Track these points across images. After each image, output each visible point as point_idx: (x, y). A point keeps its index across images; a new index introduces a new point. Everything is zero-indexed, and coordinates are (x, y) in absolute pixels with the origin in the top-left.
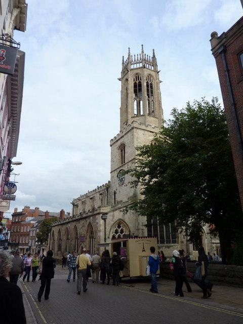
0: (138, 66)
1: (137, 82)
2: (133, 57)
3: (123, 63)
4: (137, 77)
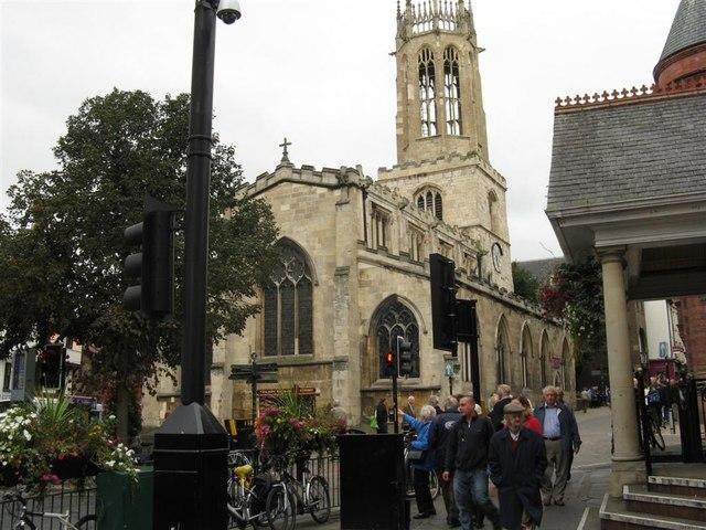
0: (427, 29)
1: (426, 63)
2: (416, 9)
3: (399, 17)
4: (426, 52)
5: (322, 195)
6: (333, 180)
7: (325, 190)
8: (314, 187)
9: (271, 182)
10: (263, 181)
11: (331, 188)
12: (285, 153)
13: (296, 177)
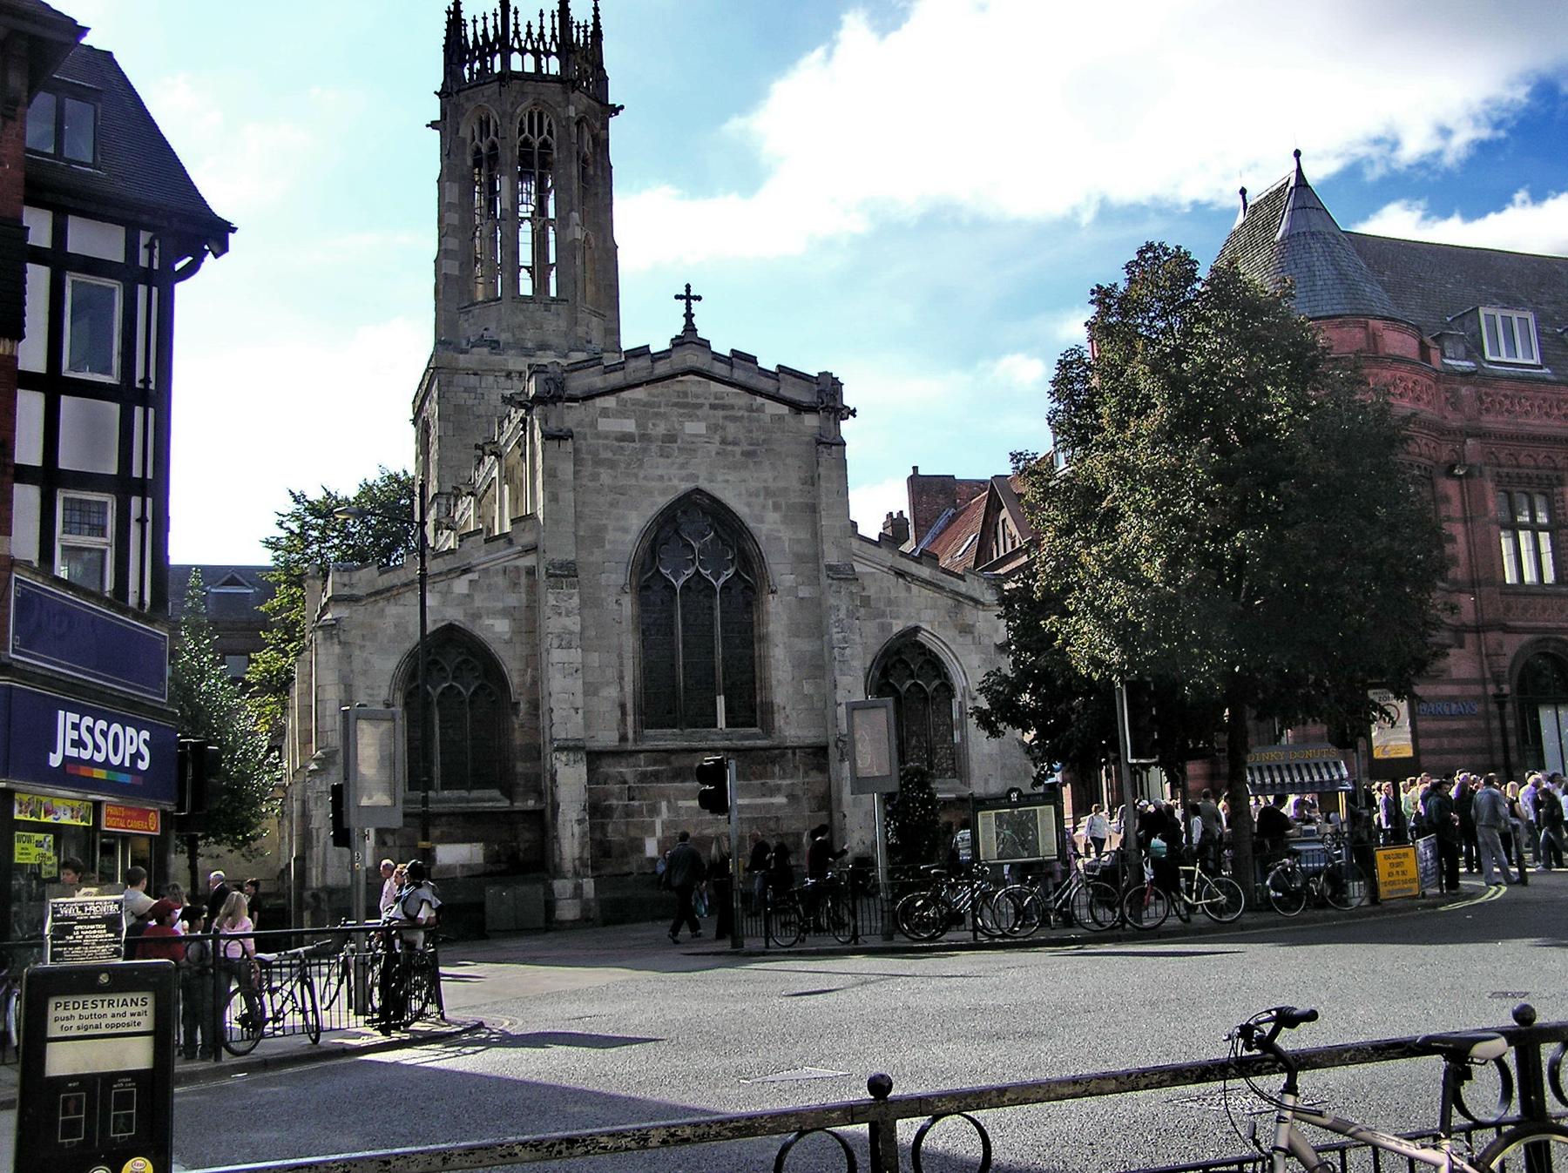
5: (781, 418)
6: (805, 397)
7: (785, 410)
8: (759, 400)
9: (662, 368)
10: (643, 362)
11: (798, 408)
12: (689, 316)
13: (720, 369)
